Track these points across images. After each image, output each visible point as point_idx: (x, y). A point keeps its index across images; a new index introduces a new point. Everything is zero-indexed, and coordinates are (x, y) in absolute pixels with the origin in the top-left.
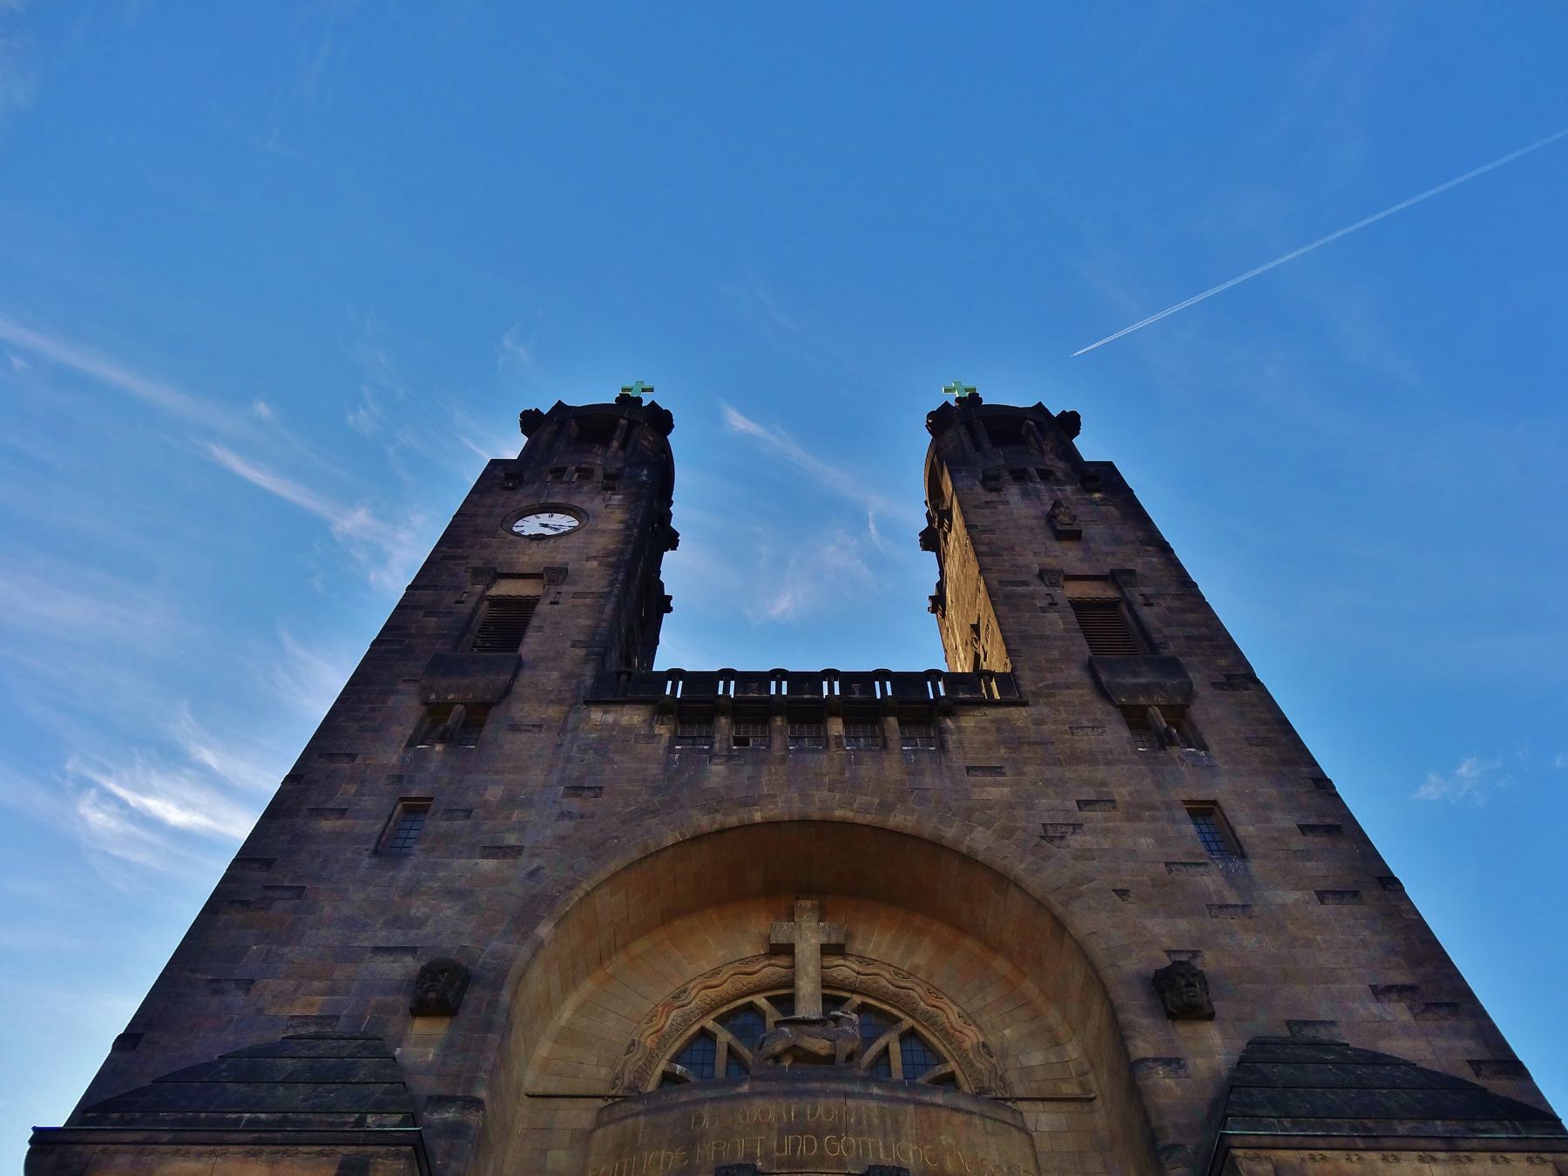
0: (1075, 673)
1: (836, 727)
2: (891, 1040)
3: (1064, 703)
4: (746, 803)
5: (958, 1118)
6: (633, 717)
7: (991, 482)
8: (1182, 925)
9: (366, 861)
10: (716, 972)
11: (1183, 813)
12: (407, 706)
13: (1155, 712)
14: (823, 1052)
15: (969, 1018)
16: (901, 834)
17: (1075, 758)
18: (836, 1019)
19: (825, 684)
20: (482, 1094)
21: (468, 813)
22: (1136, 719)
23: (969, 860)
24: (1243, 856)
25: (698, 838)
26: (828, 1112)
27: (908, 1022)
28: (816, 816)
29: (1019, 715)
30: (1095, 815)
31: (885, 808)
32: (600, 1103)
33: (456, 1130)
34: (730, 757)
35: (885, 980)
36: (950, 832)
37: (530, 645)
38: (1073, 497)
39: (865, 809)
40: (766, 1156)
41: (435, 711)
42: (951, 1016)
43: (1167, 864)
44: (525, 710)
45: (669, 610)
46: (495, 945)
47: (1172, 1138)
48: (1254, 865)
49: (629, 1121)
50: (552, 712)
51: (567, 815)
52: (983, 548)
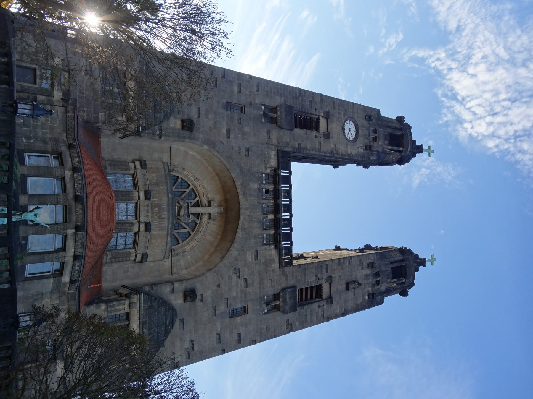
0: (292, 282)
1: (271, 217)
2: (188, 229)
3: (280, 279)
4: (244, 194)
5: (165, 244)
6: (273, 162)
7: (371, 265)
8: (210, 300)
9: (224, 101)
10: (203, 187)
11: (243, 305)
12: (277, 101)
13: (277, 303)
15: (193, 248)
16: (236, 233)
17: (261, 280)
18: (189, 216)
19: (289, 214)
20: (163, 138)
21: (240, 124)
22: (276, 297)
23: (229, 249)
24: (230, 317)
25: (234, 181)
26: (164, 214)
27: (192, 234)
28: (241, 212)
29: (276, 265)
30: (243, 282)
31: (244, 229)
32: (169, 163)
33: (154, 134)
34: (260, 189)
35: (202, 229)
36: (236, 245)
37: (299, 132)
38: (366, 290)
39: (243, 224)
40: (154, 201)
41: (274, 110)
42: (193, 244)
43: (227, 298)
44: (275, 134)
45: (334, 167)
46: (201, 136)
47: (155, 288)
48: (228, 320)
49: (163, 170)
50: (275, 141)
52: (342, 261)
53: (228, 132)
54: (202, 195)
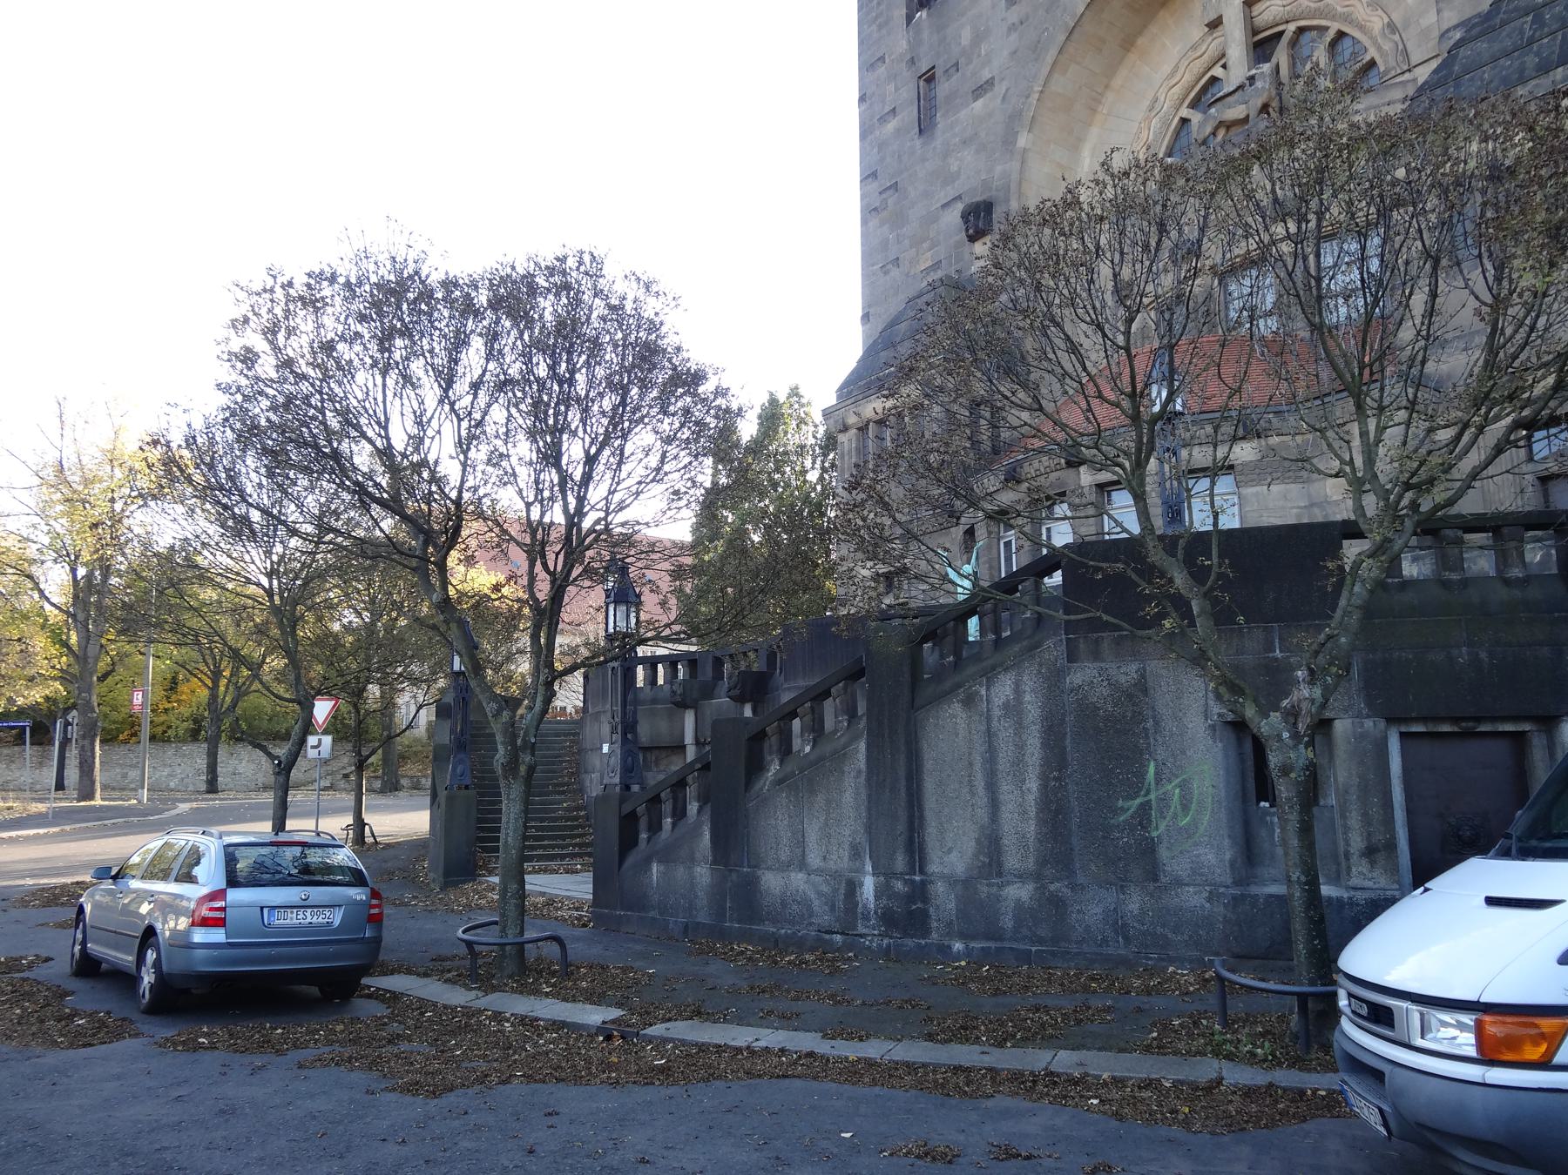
9: (918, 143)
14: (1242, 116)
46: (999, 169)
51: (1012, 28)
53: (980, 90)
54: (1198, 66)
